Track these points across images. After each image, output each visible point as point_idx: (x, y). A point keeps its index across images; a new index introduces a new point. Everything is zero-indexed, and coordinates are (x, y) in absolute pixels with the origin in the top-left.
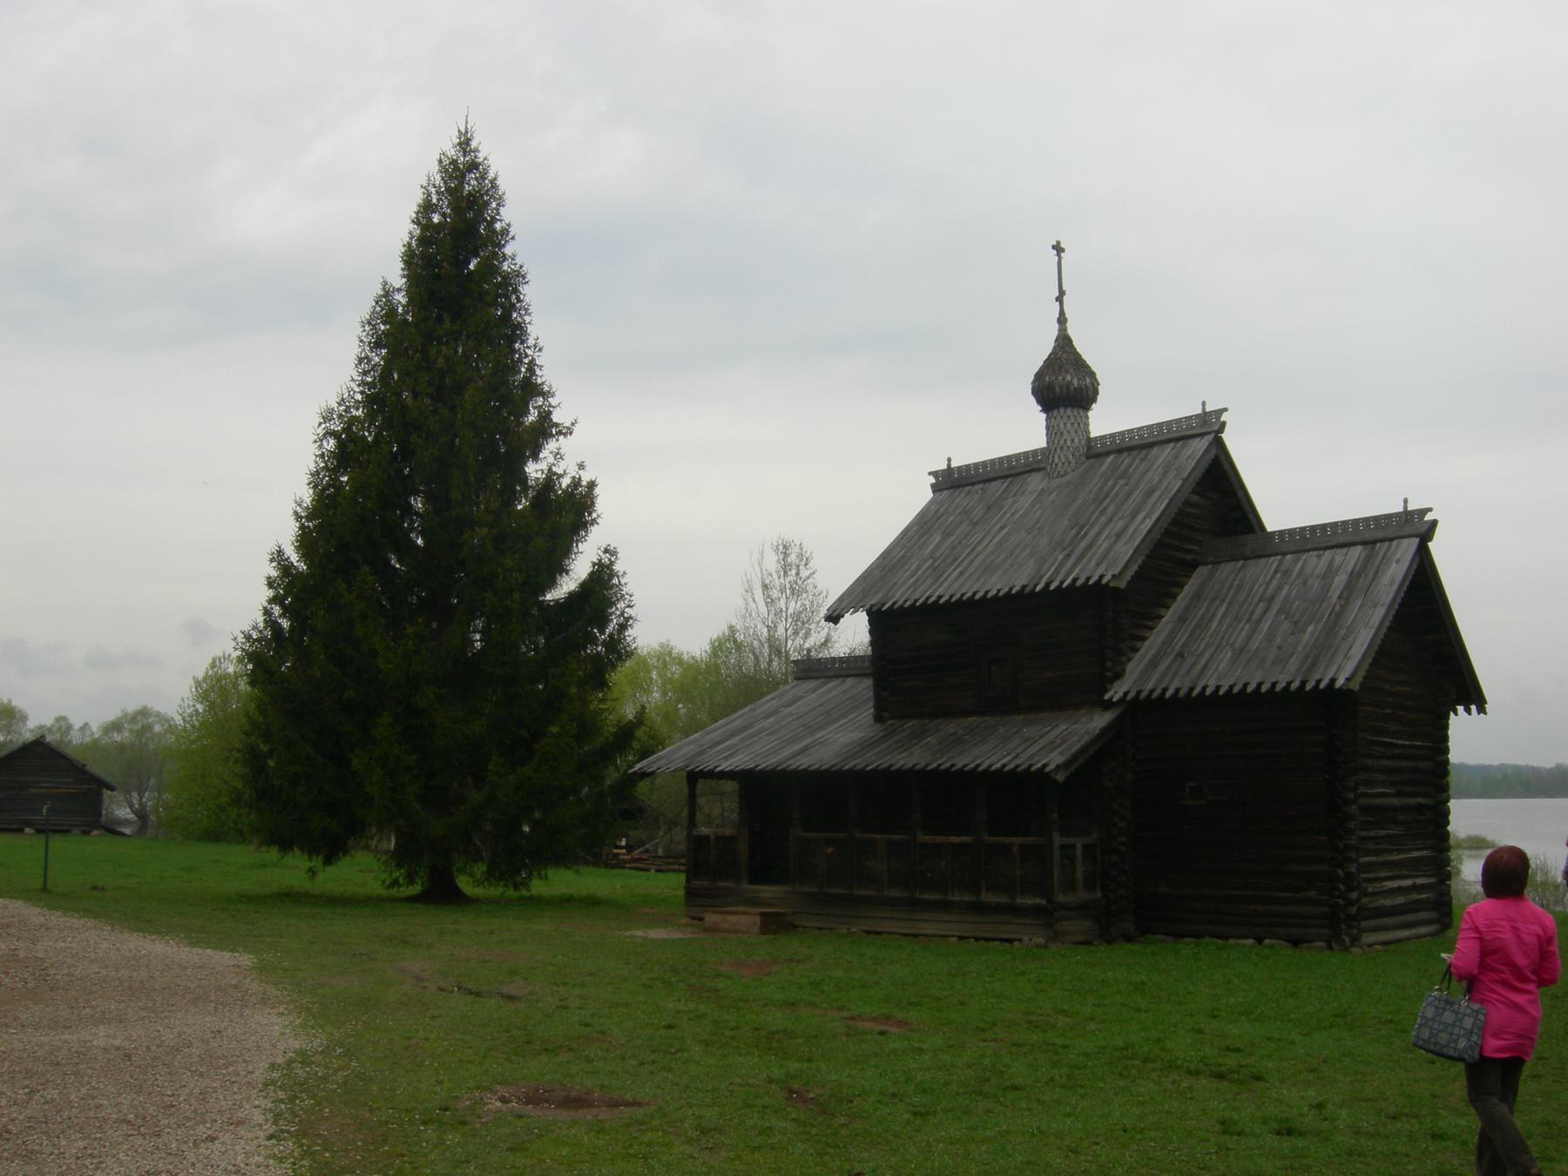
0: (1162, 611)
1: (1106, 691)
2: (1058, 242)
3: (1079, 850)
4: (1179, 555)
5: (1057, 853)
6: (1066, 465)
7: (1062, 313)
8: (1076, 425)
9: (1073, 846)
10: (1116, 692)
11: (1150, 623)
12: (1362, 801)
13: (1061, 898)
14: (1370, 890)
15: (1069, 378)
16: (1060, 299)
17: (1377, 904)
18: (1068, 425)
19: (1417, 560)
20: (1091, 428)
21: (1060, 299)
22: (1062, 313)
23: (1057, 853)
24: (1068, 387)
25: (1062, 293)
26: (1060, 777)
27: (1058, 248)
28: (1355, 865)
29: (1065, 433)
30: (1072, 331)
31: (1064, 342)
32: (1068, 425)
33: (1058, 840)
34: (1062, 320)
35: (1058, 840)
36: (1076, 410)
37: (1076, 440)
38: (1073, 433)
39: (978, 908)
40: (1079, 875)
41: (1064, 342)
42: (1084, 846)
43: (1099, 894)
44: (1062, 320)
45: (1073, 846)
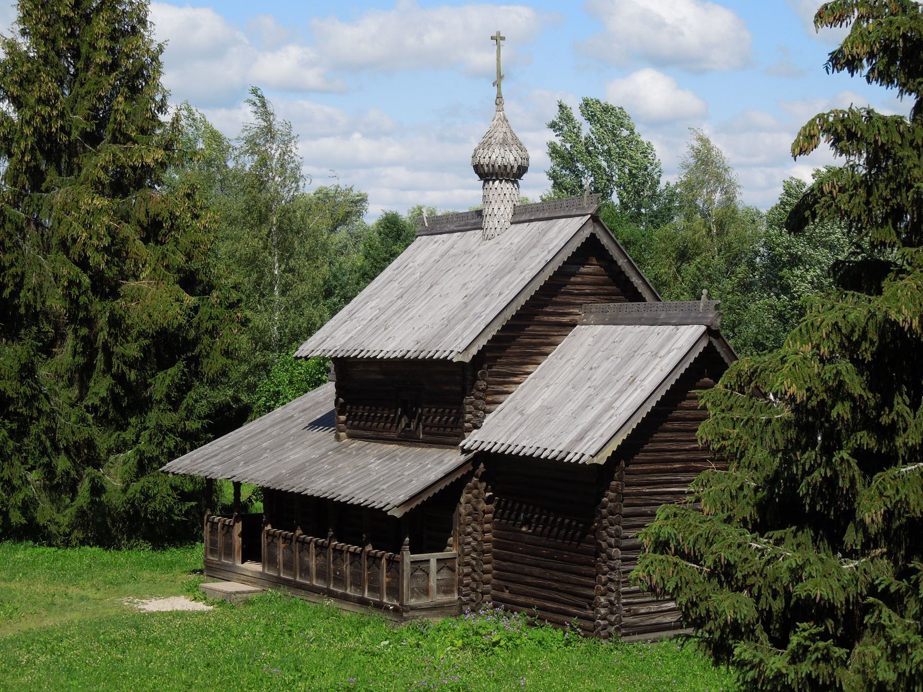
0: (530, 368)
1: (464, 438)
2: (499, 33)
3: (433, 564)
4: (553, 319)
6: (493, 229)
7: (499, 97)
9: (428, 561)
11: (516, 379)
12: (625, 543)
13: (413, 602)
14: (643, 611)
15: (494, 157)
17: (648, 622)
18: (496, 196)
19: (704, 344)
22: (499, 97)
23: (407, 569)
24: (493, 166)
27: (498, 39)
28: (614, 595)
29: (493, 202)
32: (496, 196)
33: (408, 557)
35: (408, 557)
37: (502, 208)
39: (363, 602)
40: (433, 583)
42: (438, 560)
43: (456, 597)
45: (428, 561)
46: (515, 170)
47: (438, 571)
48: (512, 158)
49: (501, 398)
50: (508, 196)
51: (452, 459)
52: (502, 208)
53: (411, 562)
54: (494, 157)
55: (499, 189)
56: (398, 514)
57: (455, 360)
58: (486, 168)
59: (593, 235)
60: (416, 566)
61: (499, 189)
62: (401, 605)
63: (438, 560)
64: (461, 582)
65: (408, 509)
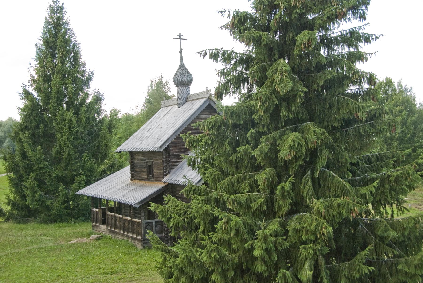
2: (180, 34)
3: (154, 224)
5: (143, 225)
8: (183, 92)
9: (152, 223)
10: (168, 179)
16: (181, 52)
20: (191, 92)
21: (181, 52)
25: (181, 50)
26: (138, 206)
30: (185, 62)
31: (182, 66)
32: (181, 92)
34: (182, 58)
36: (183, 87)
37: (183, 96)
38: (182, 94)
41: (182, 66)
42: (155, 222)
43: (164, 235)
44: (182, 58)
45: (152, 223)
46: (187, 82)
47: (156, 226)
48: (185, 78)
49: (177, 163)
50: (185, 92)
51: (160, 186)
52: (183, 96)
53: (145, 223)
54: (179, 78)
55: (182, 90)
56: (138, 206)
57: (156, 151)
58: (177, 82)
59: (210, 105)
60: (147, 224)
61: (182, 90)
62: (142, 238)
63: (155, 222)
64: (165, 229)
65: (141, 204)
